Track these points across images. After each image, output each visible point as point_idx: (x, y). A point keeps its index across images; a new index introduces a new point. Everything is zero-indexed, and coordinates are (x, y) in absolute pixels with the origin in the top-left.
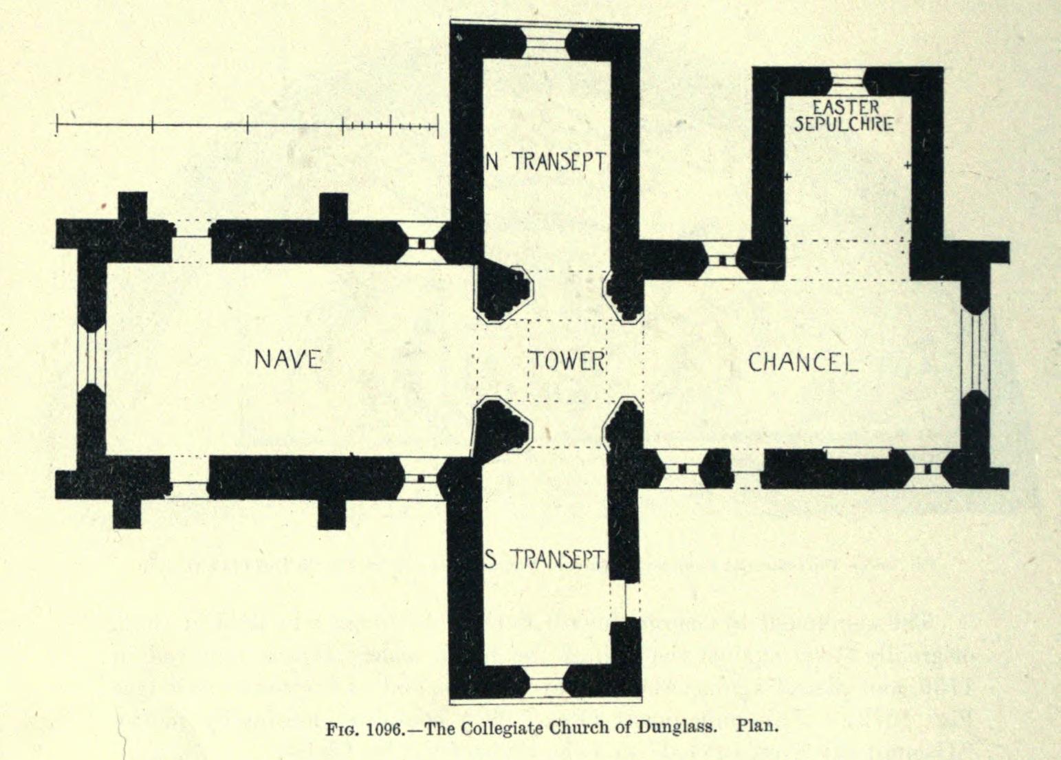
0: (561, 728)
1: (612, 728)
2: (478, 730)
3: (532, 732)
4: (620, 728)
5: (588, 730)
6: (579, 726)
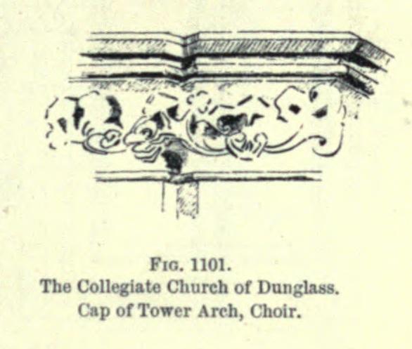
0: (179, 287)
1: (231, 288)
2: (94, 288)
3: (150, 290)
6: (198, 285)
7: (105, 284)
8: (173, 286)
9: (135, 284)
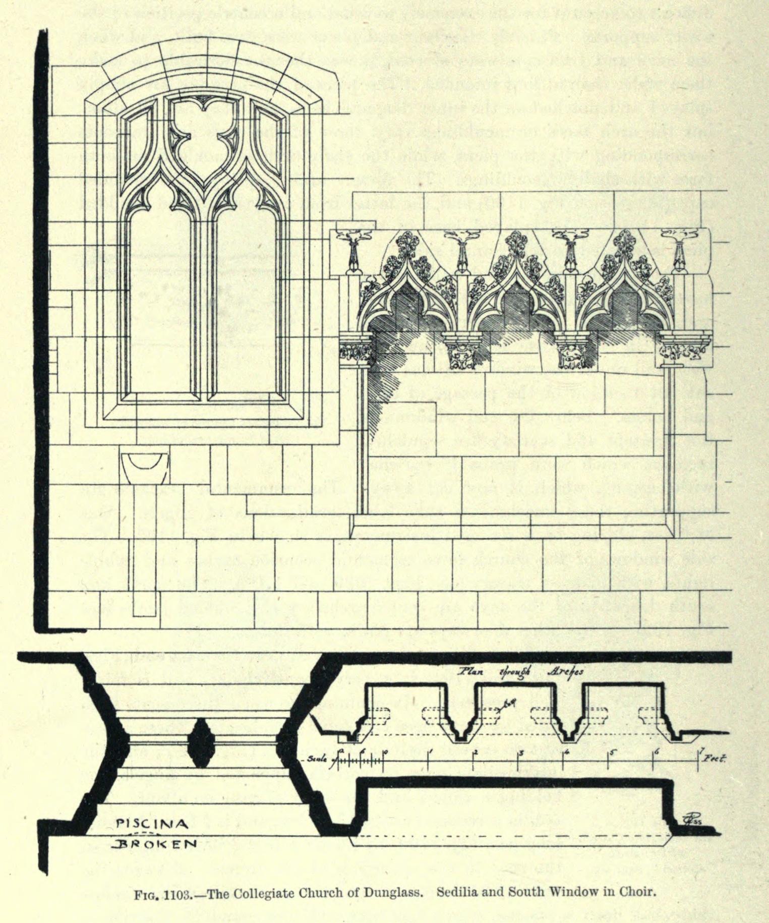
1: (345, 894)
2: (246, 895)
4: (351, 894)
5: (328, 894)
7: (254, 892)
8: (304, 893)
9: (275, 891)
